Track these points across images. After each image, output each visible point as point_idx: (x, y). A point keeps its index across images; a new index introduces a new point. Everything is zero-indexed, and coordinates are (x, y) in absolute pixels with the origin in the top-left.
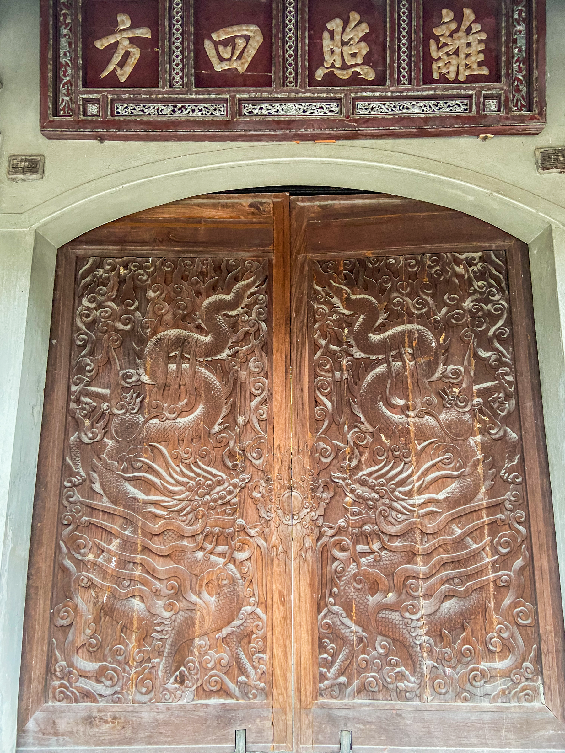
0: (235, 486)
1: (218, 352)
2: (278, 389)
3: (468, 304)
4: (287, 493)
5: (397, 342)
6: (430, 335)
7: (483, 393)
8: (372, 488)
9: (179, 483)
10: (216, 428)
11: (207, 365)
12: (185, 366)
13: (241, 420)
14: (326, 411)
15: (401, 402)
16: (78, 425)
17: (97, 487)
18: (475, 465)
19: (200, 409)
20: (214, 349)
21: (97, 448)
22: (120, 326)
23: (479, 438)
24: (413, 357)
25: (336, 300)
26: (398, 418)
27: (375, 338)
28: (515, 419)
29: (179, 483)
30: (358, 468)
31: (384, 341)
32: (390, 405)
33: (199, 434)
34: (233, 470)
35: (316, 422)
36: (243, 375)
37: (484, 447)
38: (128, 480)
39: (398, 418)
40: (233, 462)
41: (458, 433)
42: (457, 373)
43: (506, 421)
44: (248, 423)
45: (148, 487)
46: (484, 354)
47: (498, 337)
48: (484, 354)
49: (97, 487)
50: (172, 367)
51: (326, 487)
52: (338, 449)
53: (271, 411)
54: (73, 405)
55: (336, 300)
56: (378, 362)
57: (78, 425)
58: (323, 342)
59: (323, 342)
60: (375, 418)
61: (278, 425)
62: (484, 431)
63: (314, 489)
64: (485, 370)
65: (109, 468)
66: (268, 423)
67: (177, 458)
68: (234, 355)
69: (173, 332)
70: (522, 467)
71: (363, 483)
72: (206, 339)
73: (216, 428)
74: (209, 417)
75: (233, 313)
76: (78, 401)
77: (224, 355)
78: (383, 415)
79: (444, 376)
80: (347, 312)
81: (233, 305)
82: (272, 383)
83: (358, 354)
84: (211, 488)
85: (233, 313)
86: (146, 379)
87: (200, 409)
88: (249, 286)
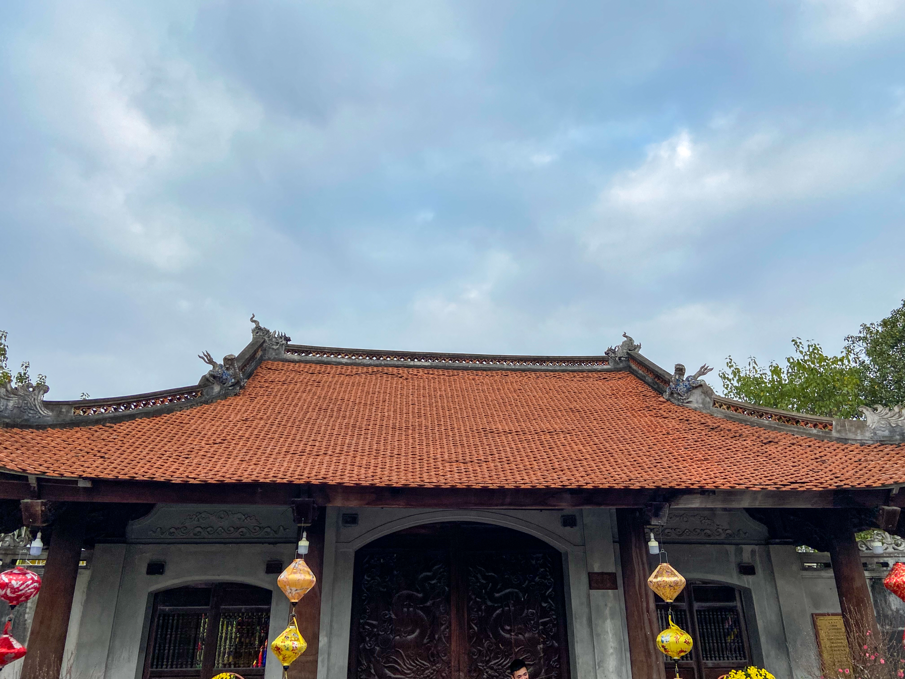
0: (434, 670)
1: (426, 602)
2: (453, 621)
3: (537, 579)
4: (457, 674)
5: (507, 596)
6: (521, 595)
7: (544, 624)
8: (495, 671)
9: (409, 669)
10: (425, 641)
11: (421, 609)
12: (411, 609)
13: (437, 636)
14: (474, 632)
15: (508, 628)
16: (364, 641)
17: (373, 671)
18: (540, 659)
19: (418, 631)
20: (424, 600)
21: (372, 651)
22: (382, 589)
23: (541, 646)
24: (514, 606)
25: (479, 576)
26: (507, 636)
27: (497, 595)
28: (555, 637)
29: (409, 669)
30: (489, 661)
31: (501, 597)
32: (504, 630)
33: (418, 643)
34: (433, 663)
35: (470, 638)
36: (437, 614)
37: (544, 650)
38: (386, 667)
39: (507, 636)
40: (433, 658)
41: (533, 642)
42: (532, 614)
43: (553, 638)
44: (440, 638)
45: (394, 670)
46: (544, 605)
47: (550, 596)
48: (544, 605)
49: (373, 671)
50: (405, 609)
51: (475, 671)
52: (480, 651)
53: (450, 631)
54: (361, 630)
55: (479, 576)
56: (499, 607)
57: (364, 641)
58: (473, 597)
59: (473, 597)
60: (497, 636)
61: (454, 639)
62: (544, 643)
63: (470, 672)
64: (544, 613)
65: (378, 662)
66: (449, 639)
67: (408, 657)
68: (433, 604)
69: (405, 592)
70: (558, 661)
71: (492, 668)
72: (420, 595)
73: (425, 641)
74: (422, 635)
75: (433, 582)
76: (364, 628)
77: (428, 604)
78: (500, 634)
79: (527, 615)
80: (484, 582)
81: (431, 578)
82: (450, 618)
83: (489, 603)
84: (424, 671)
85: (433, 582)
86: (393, 616)
87: (418, 631)
88: (439, 568)
